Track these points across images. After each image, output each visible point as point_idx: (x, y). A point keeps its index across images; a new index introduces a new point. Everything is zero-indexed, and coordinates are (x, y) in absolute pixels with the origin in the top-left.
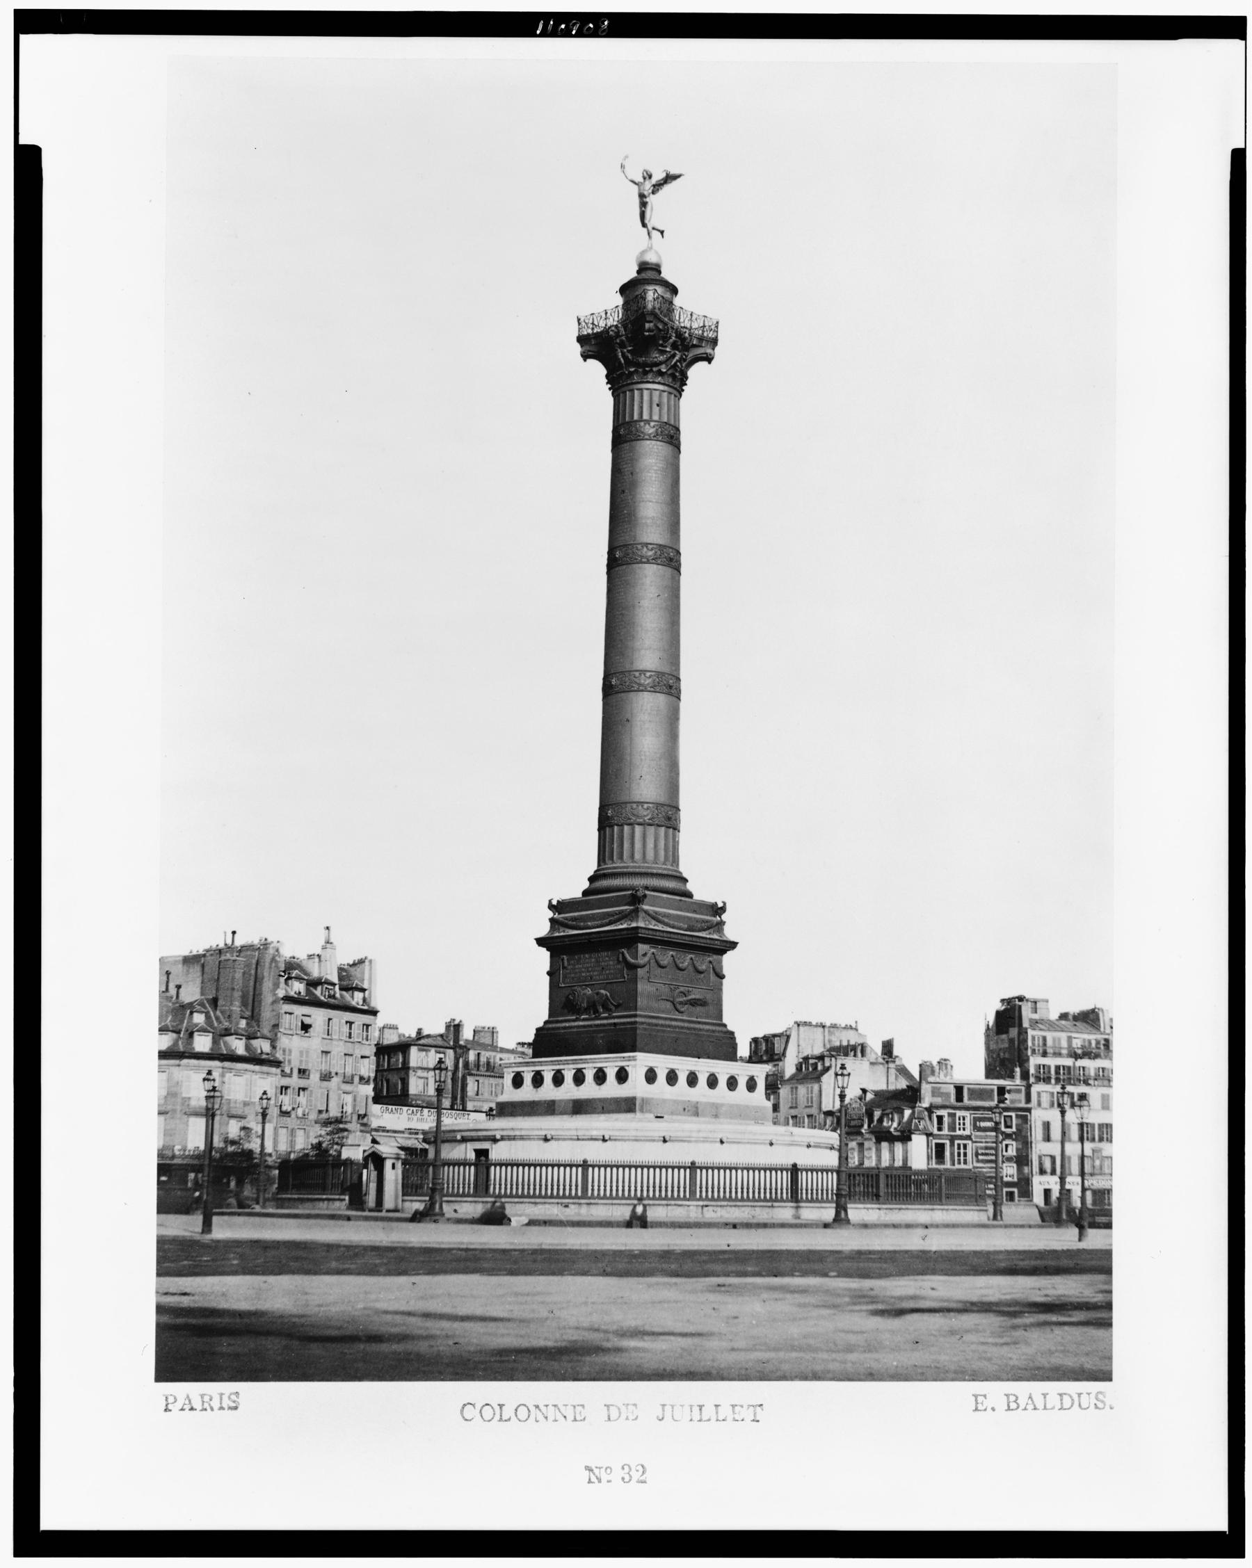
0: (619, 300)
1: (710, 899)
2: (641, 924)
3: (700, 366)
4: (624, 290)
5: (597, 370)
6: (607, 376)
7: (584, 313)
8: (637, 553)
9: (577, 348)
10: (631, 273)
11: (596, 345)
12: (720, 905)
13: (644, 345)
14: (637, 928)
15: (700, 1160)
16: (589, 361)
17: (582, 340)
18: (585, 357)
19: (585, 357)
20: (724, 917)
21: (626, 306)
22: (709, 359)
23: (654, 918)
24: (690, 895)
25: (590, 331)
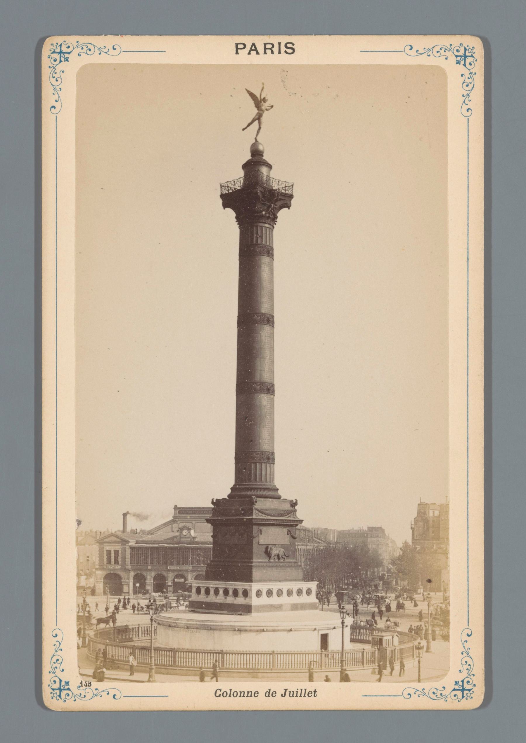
0: (241, 173)
1: (290, 498)
2: (254, 517)
3: (284, 211)
4: (244, 167)
5: (231, 214)
6: (236, 218)
7: (223, 181)
8: (252, 319)
9: (220, 201)
10: (248, 157)
11: (229, 199)
12: (294, 501)
13: (254, 203)
14: (252, 519)
15: (278, 649)
16: (227, 209)
17: (222, 196)
18: (225, 206)
19: (225, 206)
20: (296, 507)
21: (246, 177)
22: (289, 207)
23: (262, 513)
24: (279, 497)
25: (227, 192)
